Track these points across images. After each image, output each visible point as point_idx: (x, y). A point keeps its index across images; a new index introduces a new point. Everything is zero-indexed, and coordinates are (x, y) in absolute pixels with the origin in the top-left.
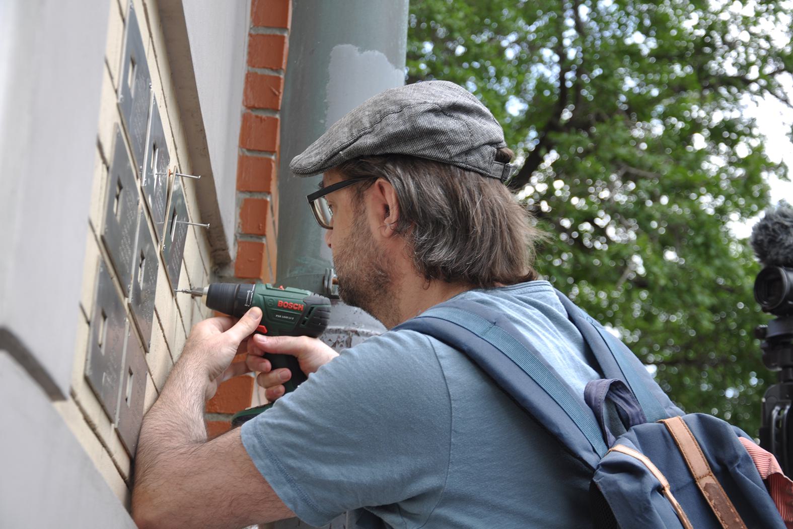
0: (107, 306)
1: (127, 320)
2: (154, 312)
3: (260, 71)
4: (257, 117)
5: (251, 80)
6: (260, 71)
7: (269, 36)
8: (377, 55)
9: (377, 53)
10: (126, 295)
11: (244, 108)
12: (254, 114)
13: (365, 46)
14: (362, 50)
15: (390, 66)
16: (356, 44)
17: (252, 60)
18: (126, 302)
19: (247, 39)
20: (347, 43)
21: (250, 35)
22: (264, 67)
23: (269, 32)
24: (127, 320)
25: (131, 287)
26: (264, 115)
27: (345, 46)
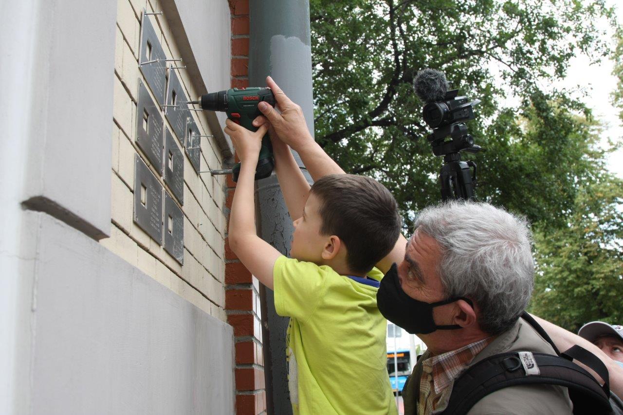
0: (144, 180)
1: (164, 189)
2: (184, 184)
3: (238, 57)
4: (239, 80)
5: (234, 63)
6: (238, 57)
7: (242, 39)
8: (294, 40)
9: (295, 38)
10: (161, 176)
11: (232, 77)
12: (237, 79)
13: (288, 35)
14: (287, 37)
15: (303, 44)
16: (283, 34)
17: (234, 52)
18: (162, 179)
19: (230, 42)
20: (279, 34)
21: (232, 40)
22: (240, 55)
23: (241, 37)
24: (164, 189)
25: (164, 171)
26: (242, 79)
27: (278, 36)
